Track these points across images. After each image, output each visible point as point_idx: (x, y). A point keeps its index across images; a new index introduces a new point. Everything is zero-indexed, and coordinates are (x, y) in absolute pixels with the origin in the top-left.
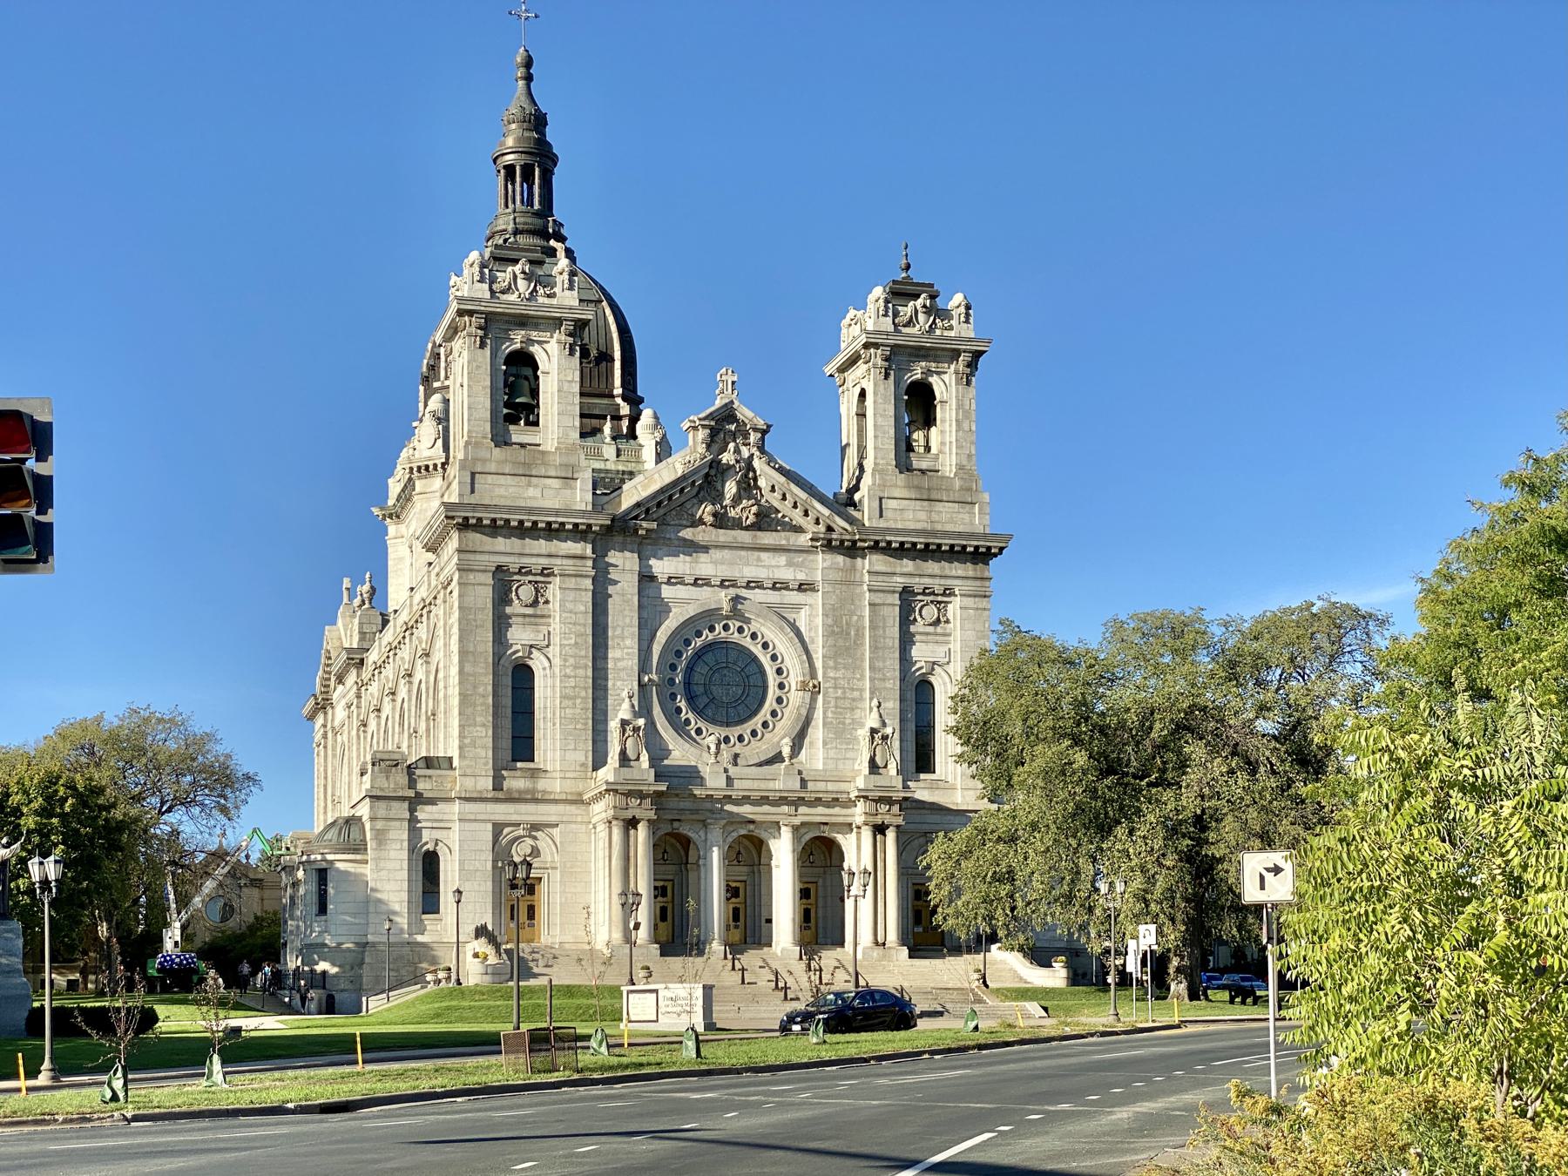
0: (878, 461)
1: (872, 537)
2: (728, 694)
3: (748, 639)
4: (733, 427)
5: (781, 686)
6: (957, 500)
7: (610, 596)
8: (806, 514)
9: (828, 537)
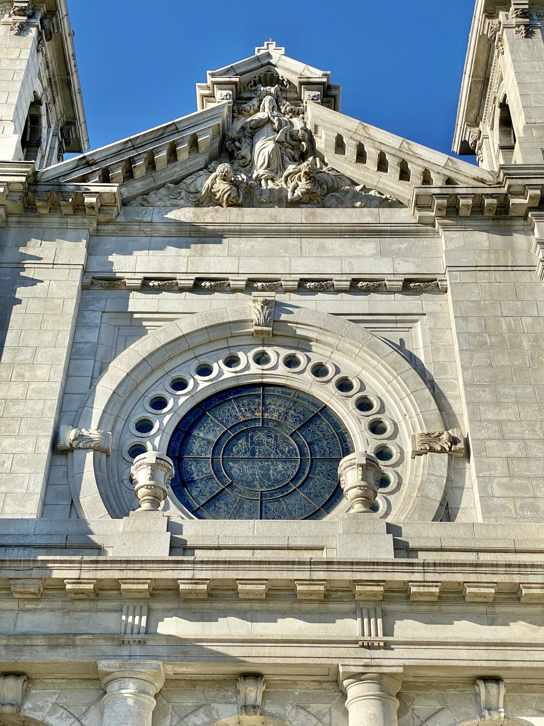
0: (533, 121)
1: (534, 182)
2: (266, 476)
3: (308, 375)
4: (273, 90)
7: (19, 302)
8: (404, 175)
9: (450, 191)
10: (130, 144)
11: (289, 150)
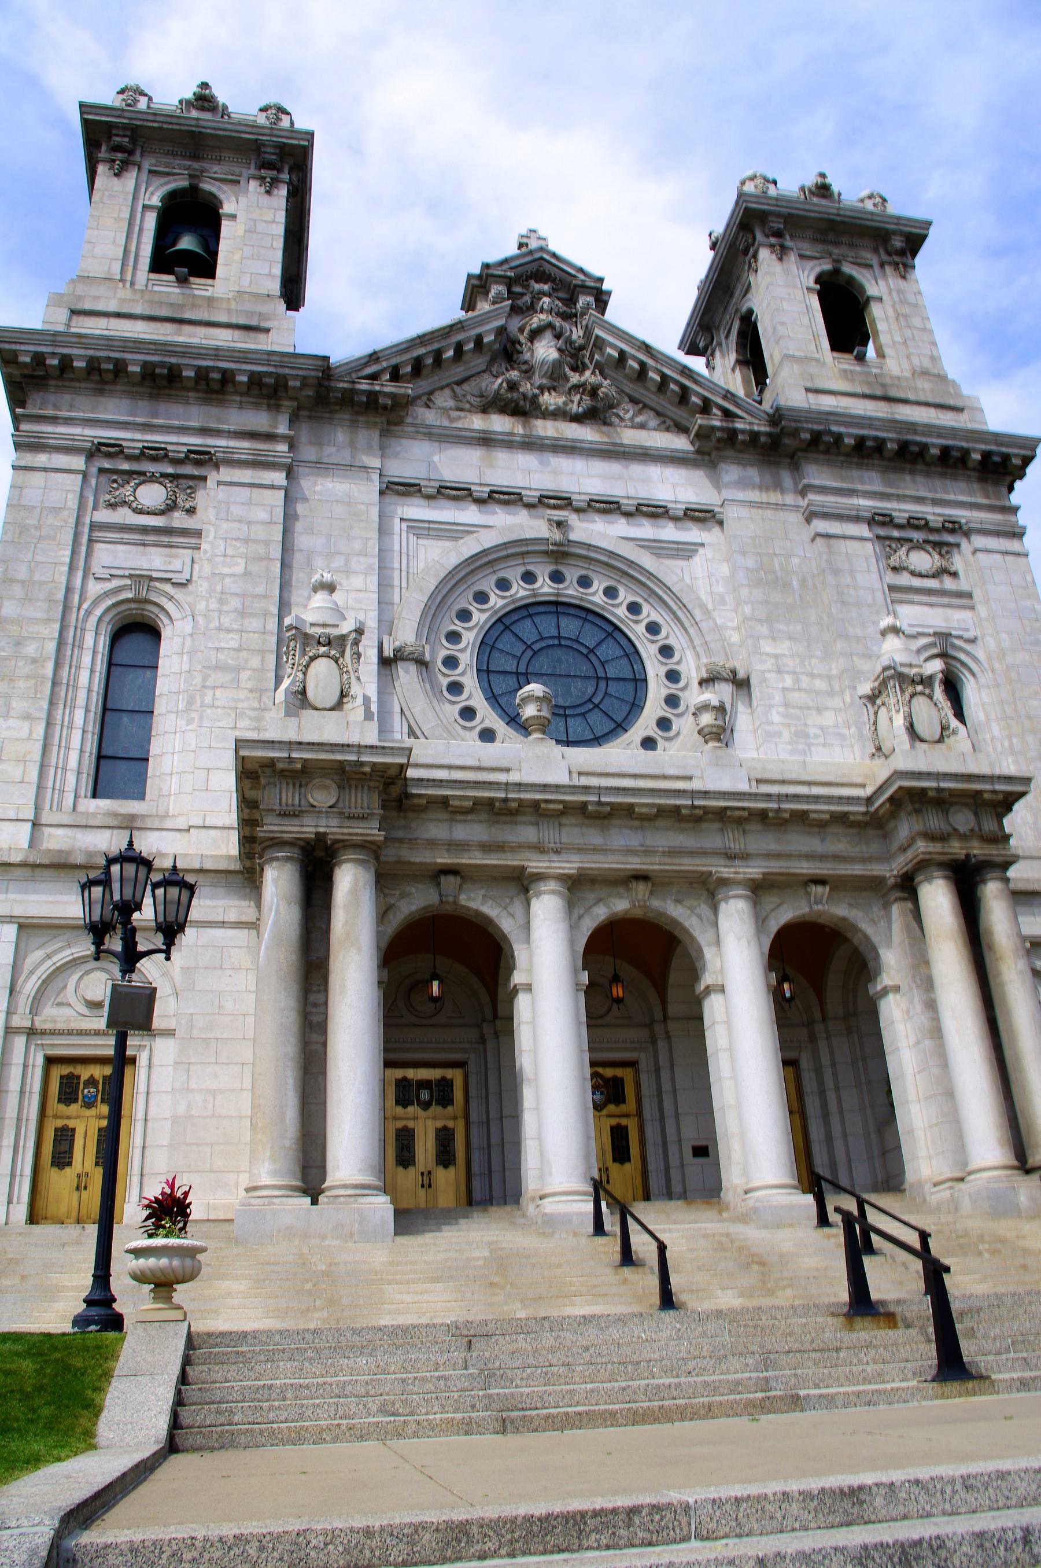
1: (805, 425)
5: (673, 676)
6: (931, 400)
9: (730, 425)
10: (418, 341)
11: (569, 359)
